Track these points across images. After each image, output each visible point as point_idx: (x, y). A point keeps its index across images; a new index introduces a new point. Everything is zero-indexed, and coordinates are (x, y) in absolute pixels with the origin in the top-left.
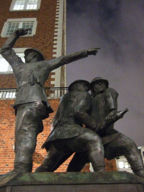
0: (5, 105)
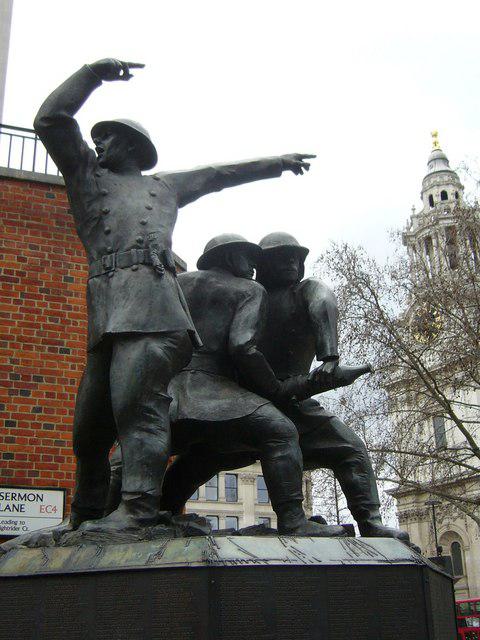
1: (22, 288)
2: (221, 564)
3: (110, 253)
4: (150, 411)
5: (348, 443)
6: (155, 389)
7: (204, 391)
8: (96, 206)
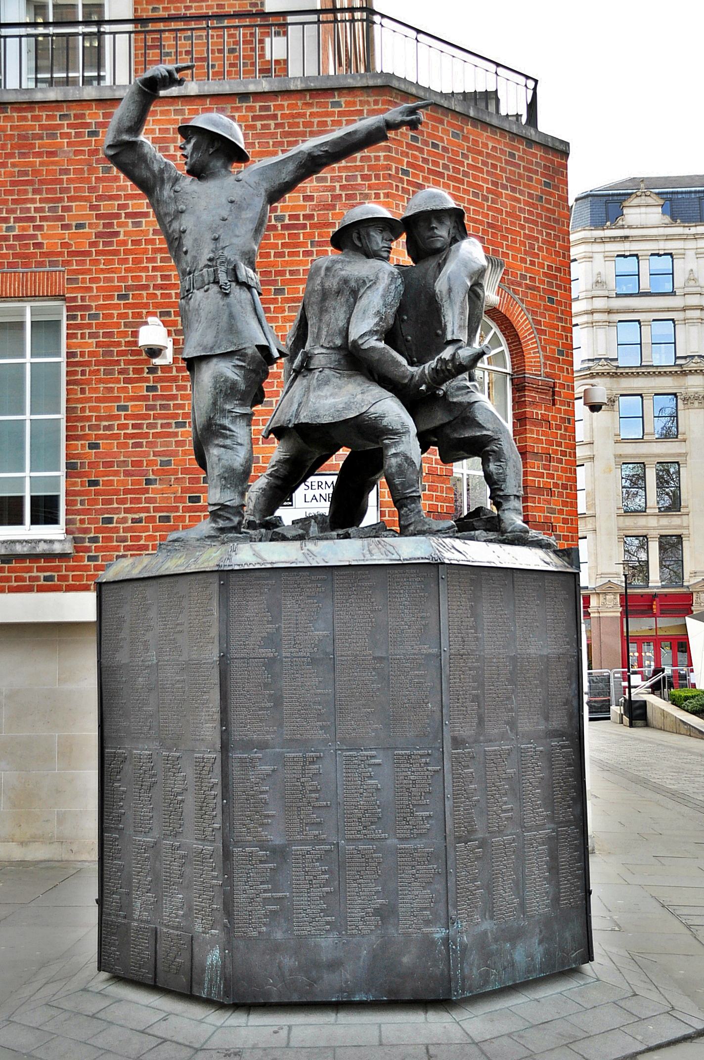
0: (60, 126)
1: (312, 235)
2: (230, 568)
3: (190, 273)
4: (225, 428)
5: (488, 430)
6: (228, 407)
7: (326, 391)
8: (175, 225)
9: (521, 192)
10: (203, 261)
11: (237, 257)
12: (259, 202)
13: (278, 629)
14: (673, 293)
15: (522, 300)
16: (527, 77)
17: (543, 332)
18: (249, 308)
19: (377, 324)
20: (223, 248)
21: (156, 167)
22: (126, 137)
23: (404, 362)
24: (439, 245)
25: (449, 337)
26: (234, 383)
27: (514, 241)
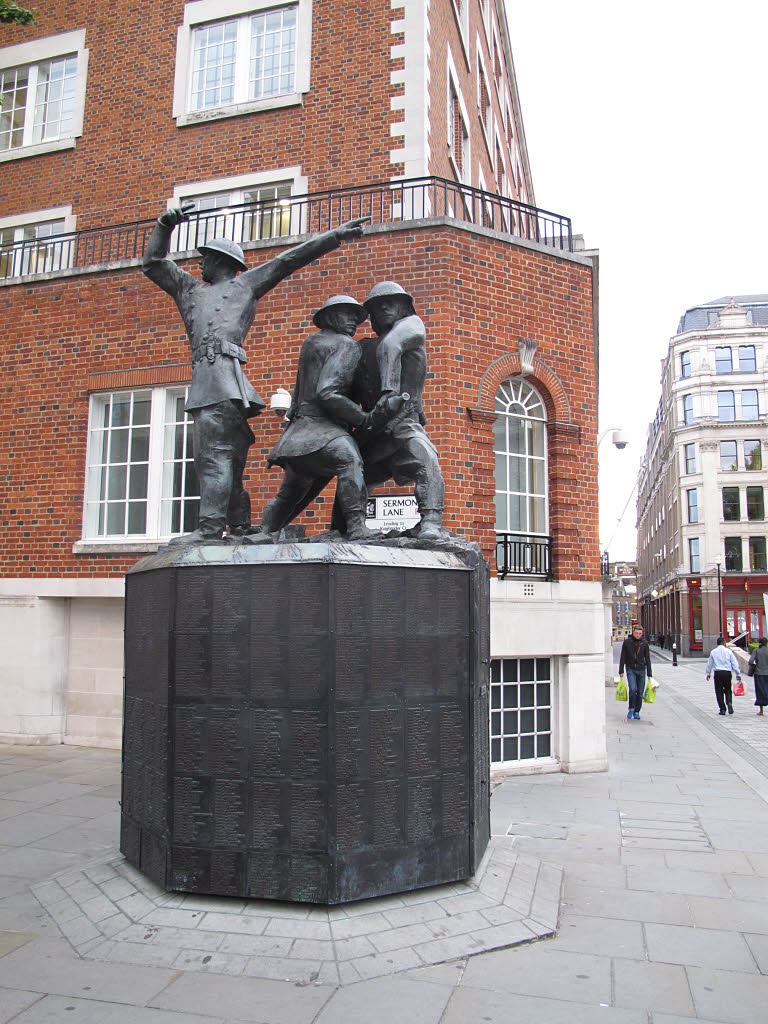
4: (209, 461)
7: (304, 432)
9: (553, 294)
10: (201, 341)
11: (224, 336)
12: (247, 297)
13: (211, 613)
14: (755, 372)
15: (554, 370)
16: (561, 217)
17: (571, 392)
18: (229, 373)
19: (335, 382)
20: (215, 331)
21: (177, 279)
22: (153, 259)
23: (359, 408)
24: (389, 321)
25: (383, 389)
26: (214, 429)
27: (546, 327)
